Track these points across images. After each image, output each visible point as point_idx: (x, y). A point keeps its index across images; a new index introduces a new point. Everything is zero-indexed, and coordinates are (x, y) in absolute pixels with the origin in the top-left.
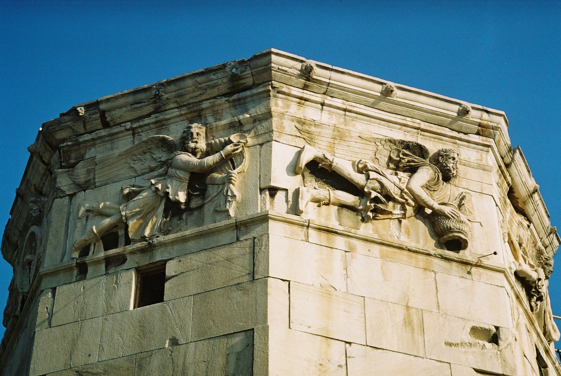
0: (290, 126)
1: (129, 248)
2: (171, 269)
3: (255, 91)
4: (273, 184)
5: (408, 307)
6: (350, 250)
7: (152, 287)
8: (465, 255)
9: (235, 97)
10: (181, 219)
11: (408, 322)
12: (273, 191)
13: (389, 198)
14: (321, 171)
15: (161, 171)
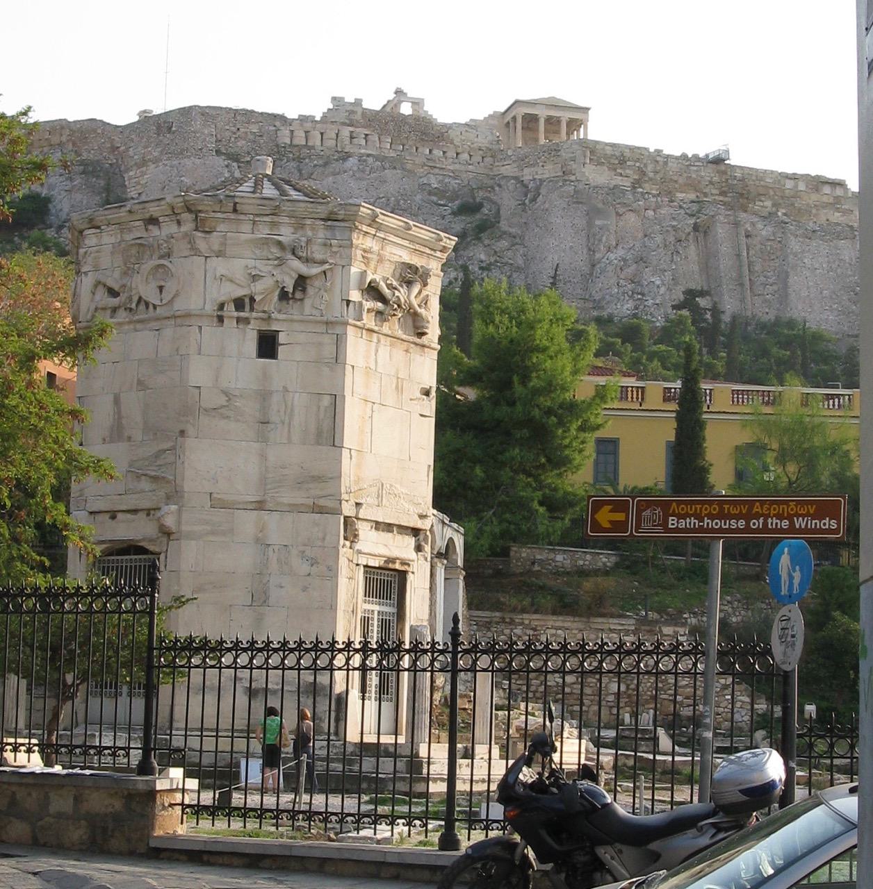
0: (359, 253)
1: (254, 314)
2: (282, 338)
3: (342, 224)
4: (350, 299)
5: (398, 378)
6: (379, 341)
7: (268, 346)
8: (424, 340)
9: (329, 223)
10: (288, 304)
11: (397, 388)
12: (348, 302)
13: (399, 306)
14: (373, 291)
15: (276, 262)
